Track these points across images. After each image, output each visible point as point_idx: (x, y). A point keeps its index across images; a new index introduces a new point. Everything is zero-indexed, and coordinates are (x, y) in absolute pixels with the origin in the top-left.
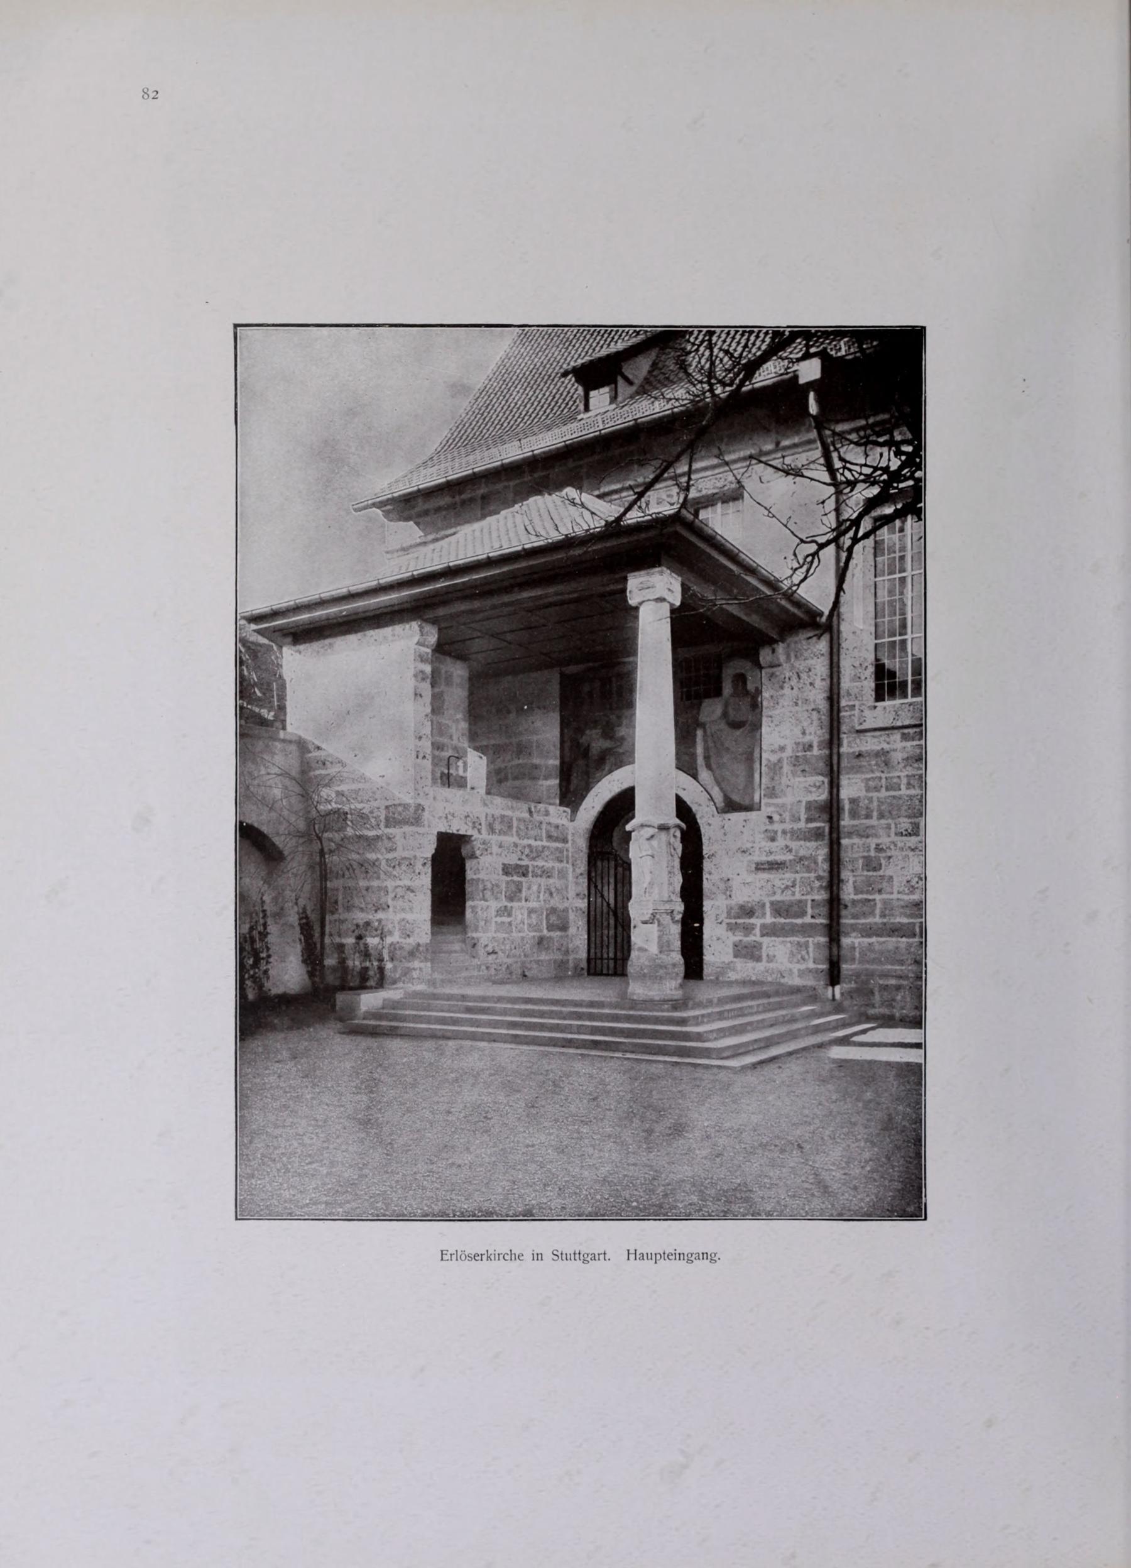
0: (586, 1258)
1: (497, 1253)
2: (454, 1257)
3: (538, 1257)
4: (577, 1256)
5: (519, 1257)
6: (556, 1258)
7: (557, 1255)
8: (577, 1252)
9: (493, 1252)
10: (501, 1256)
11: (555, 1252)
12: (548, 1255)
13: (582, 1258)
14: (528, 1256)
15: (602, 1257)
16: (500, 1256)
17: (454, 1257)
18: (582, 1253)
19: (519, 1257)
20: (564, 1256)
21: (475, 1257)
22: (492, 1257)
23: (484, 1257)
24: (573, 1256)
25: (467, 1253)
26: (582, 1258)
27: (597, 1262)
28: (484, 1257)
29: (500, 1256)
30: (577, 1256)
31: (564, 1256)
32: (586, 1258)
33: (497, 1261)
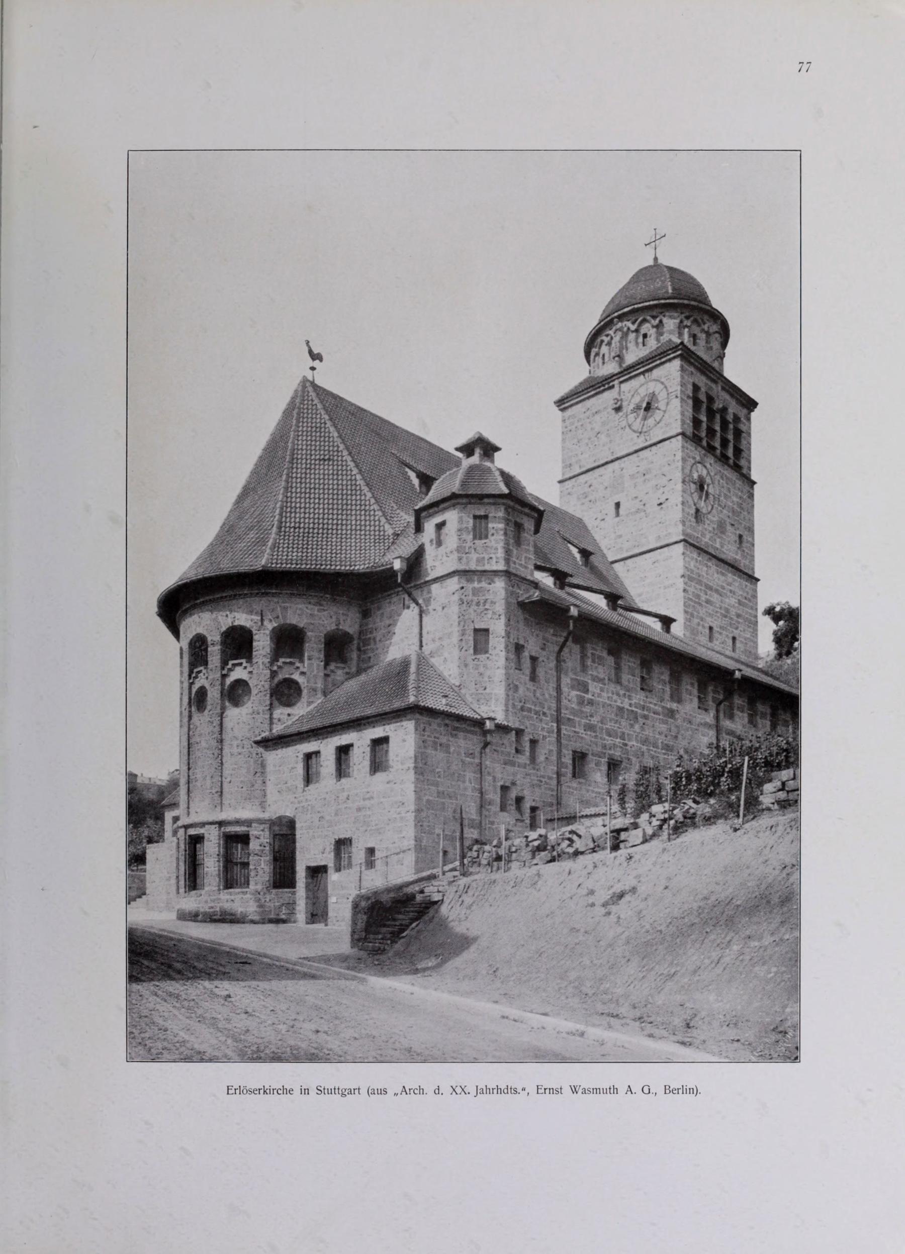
1: (271, 1088)
2: (238, 1091)
3: (305, 1091)
4: (337, 1091)
5: (290, 1091)
6: (319, 1092)
8: (337, 1088)
10: (275, 1091)
11: (319, 1088)
12: (313, 1092)
13: (340, 1092)
14: (297, 1091)
15: (357, 1091)
17: (238, 1091)
18: (341, 1088)
19: (290, 1091)
20: (326, 1091)
22: (268, 1091)
24: (333, 1090)
26: (340, 1092)
28: (262, 1091)
30: (337, 1091)
31: (326, 1091)
33: (271, 1095)
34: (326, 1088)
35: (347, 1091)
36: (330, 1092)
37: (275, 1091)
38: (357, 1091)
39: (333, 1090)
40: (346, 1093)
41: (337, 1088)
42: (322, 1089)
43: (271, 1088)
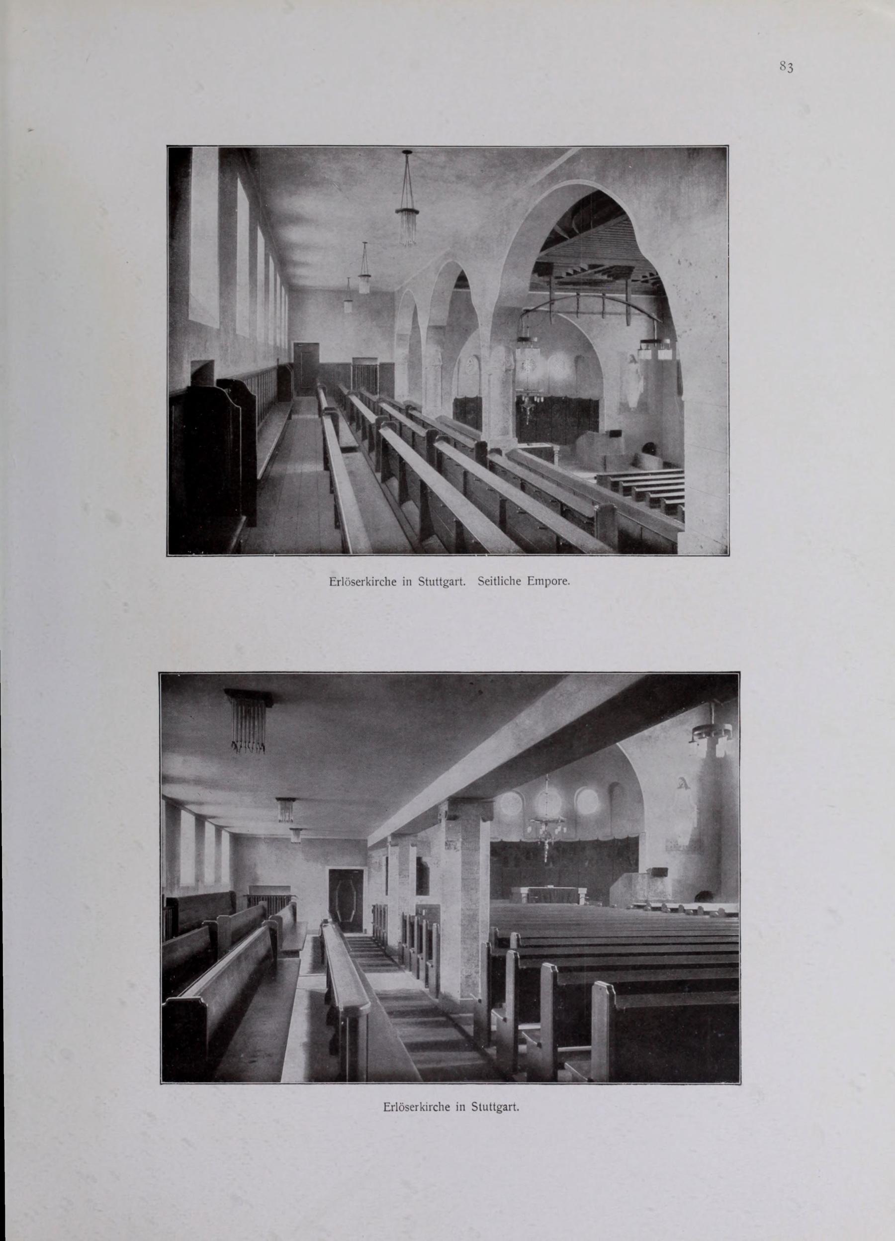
0: (447, 584)
1: (374, 580)
4: (439, 582)
6: (422, 583)
7: (423, 581)
8: (439, 579)
9: (372, 579)
10: (378, 582)
11: (421, 579)
12: (415, 582)
13: (443, 583)
15: (458, 582)
16: (376, 582)
17: (341, 583)
20: (428, 582)
21: (355, 583)
23: (365, 583)
24: (435, 582)
25: (350, 580)
26: (443, 583)
27: (455, 586)
28: (365, 583)
29: (376, 582)
30: (439, 582)
31: (428, 582)
32: (447, 584)
35: (449, 582)
36: (433, 583)
37: (378, 582)
39: (435, 582)
43: (374, 580)
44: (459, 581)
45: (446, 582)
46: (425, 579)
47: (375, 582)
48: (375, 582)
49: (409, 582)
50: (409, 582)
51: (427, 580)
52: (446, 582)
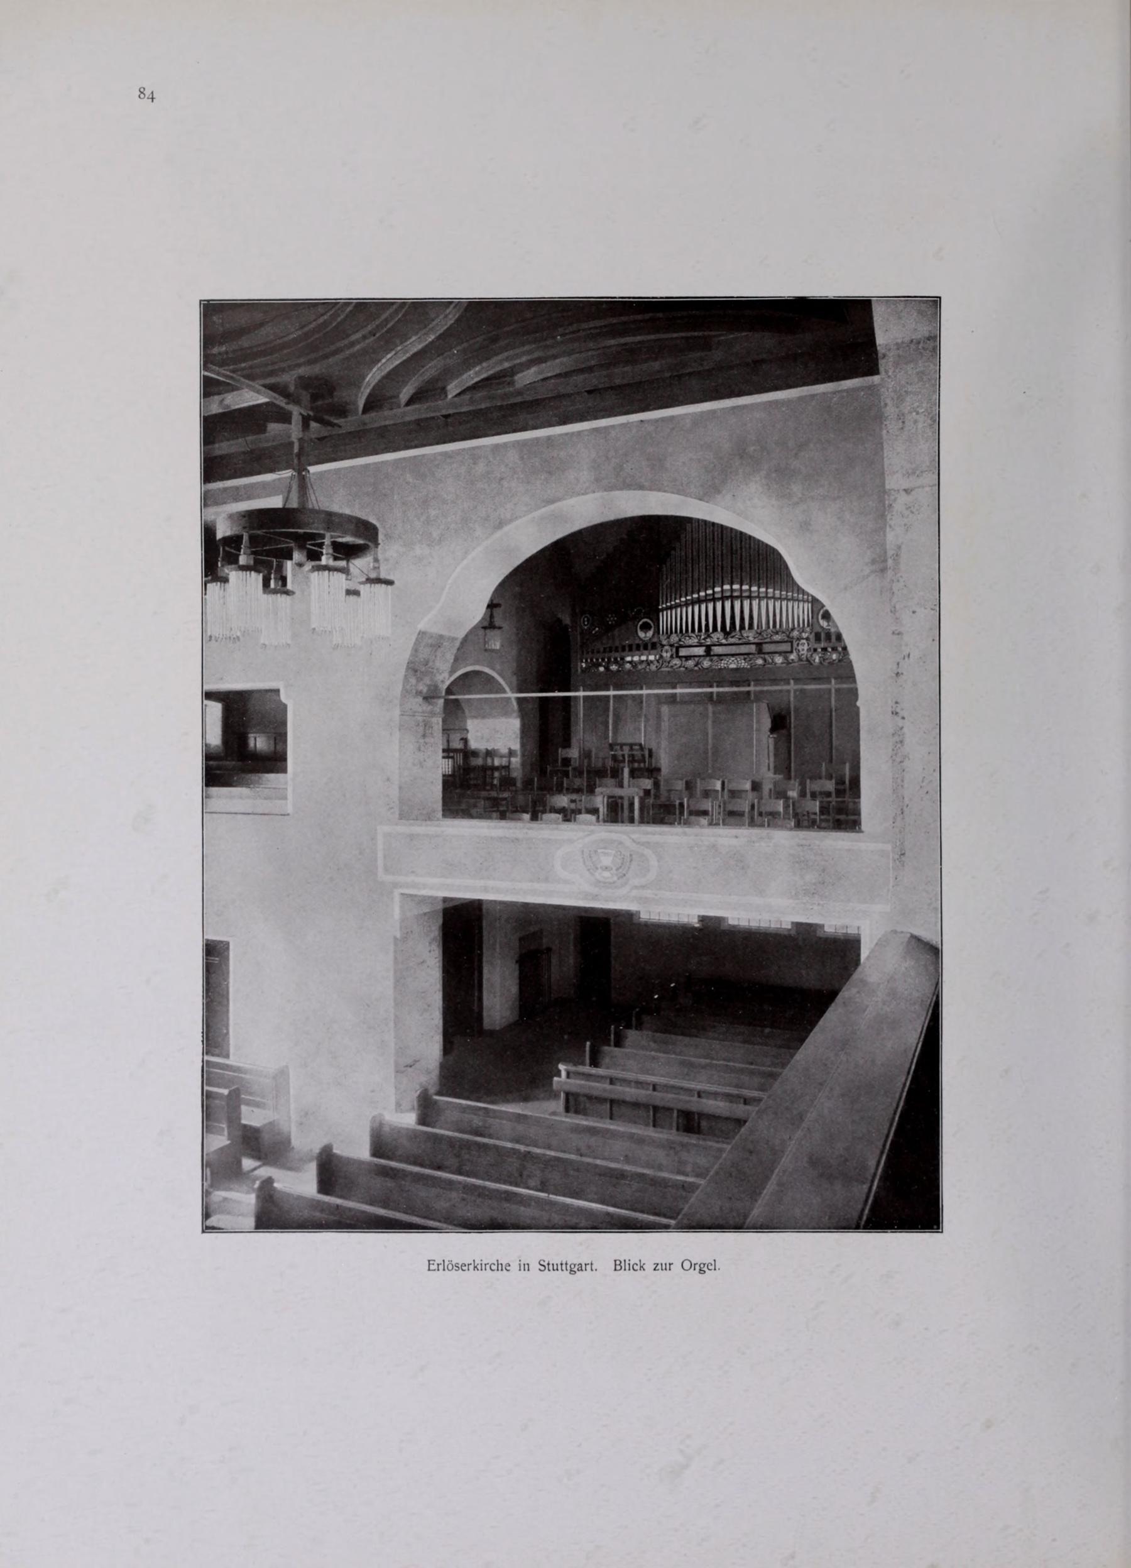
1: (484, 1263)
2: (441, 1267)
4: (564, 1266)
5: (506, 1267)
6: (542, 1268)
7: (544, 1266)
8: (564, 1262)
9: (480, 1262)
10: (488, 1267)
11: (542, 1263)
12: (535, 1266)
13: (569, 1268)
14: (514, 1267)
15: (589, 1267)
17: (441, 1267)
18: (569, 1263)
19: (506, 1267)
22: (479, 1267)
25: (454, 1263)
27: (584, 1272)
28: (471, 1267)
30: (564, 1266)
34: (551, 1263)
35: (577, 1267)
38: (589, 1267)
40: (576, 1269)
41: (564, 1262)
42: (545, 1264)
44: (590, 1266)
45: (573, 1266)
46: (547, 1262)
47: (483, 1266)
48: (483, 1266)
49: (526, 1266)
50: (526, 1266)
51: (548, 1264)
52: (573, 1266)
